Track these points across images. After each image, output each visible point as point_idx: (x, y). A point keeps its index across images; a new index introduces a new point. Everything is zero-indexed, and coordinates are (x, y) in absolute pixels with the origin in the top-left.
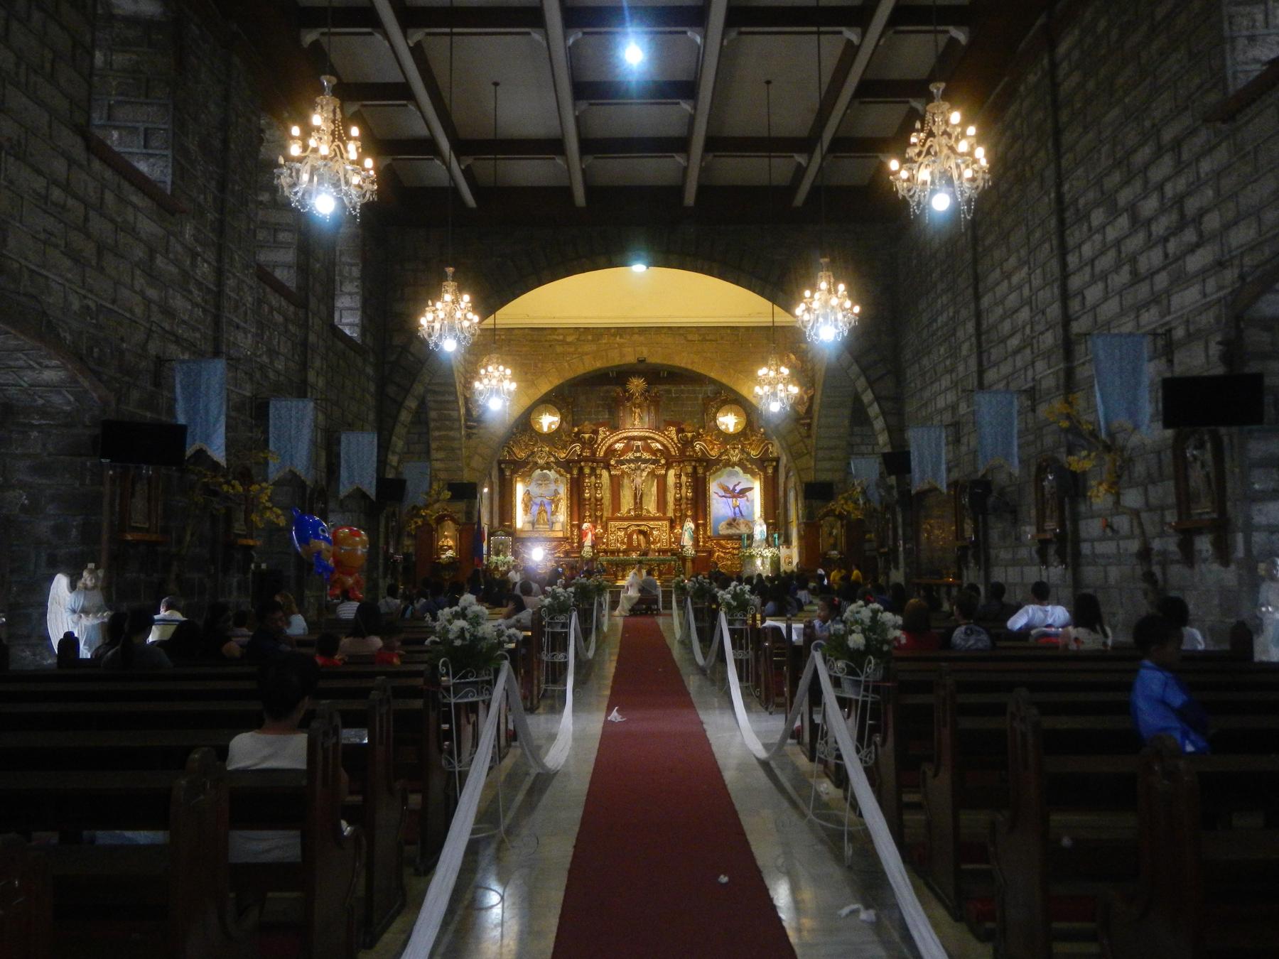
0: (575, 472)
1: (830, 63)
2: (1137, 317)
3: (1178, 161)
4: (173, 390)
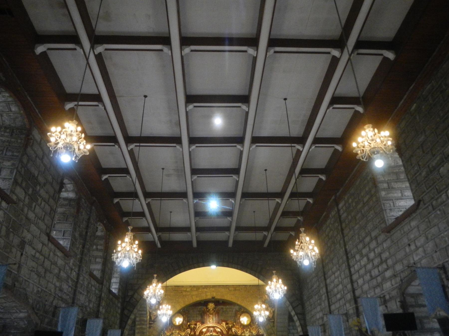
1: (272, 210)
2: (374, 290)
3: (377, 243)
4: (58, 318)
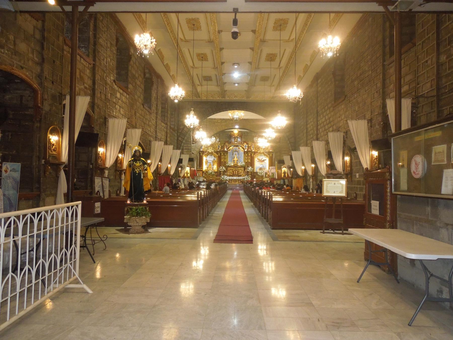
0: (219, 154)
